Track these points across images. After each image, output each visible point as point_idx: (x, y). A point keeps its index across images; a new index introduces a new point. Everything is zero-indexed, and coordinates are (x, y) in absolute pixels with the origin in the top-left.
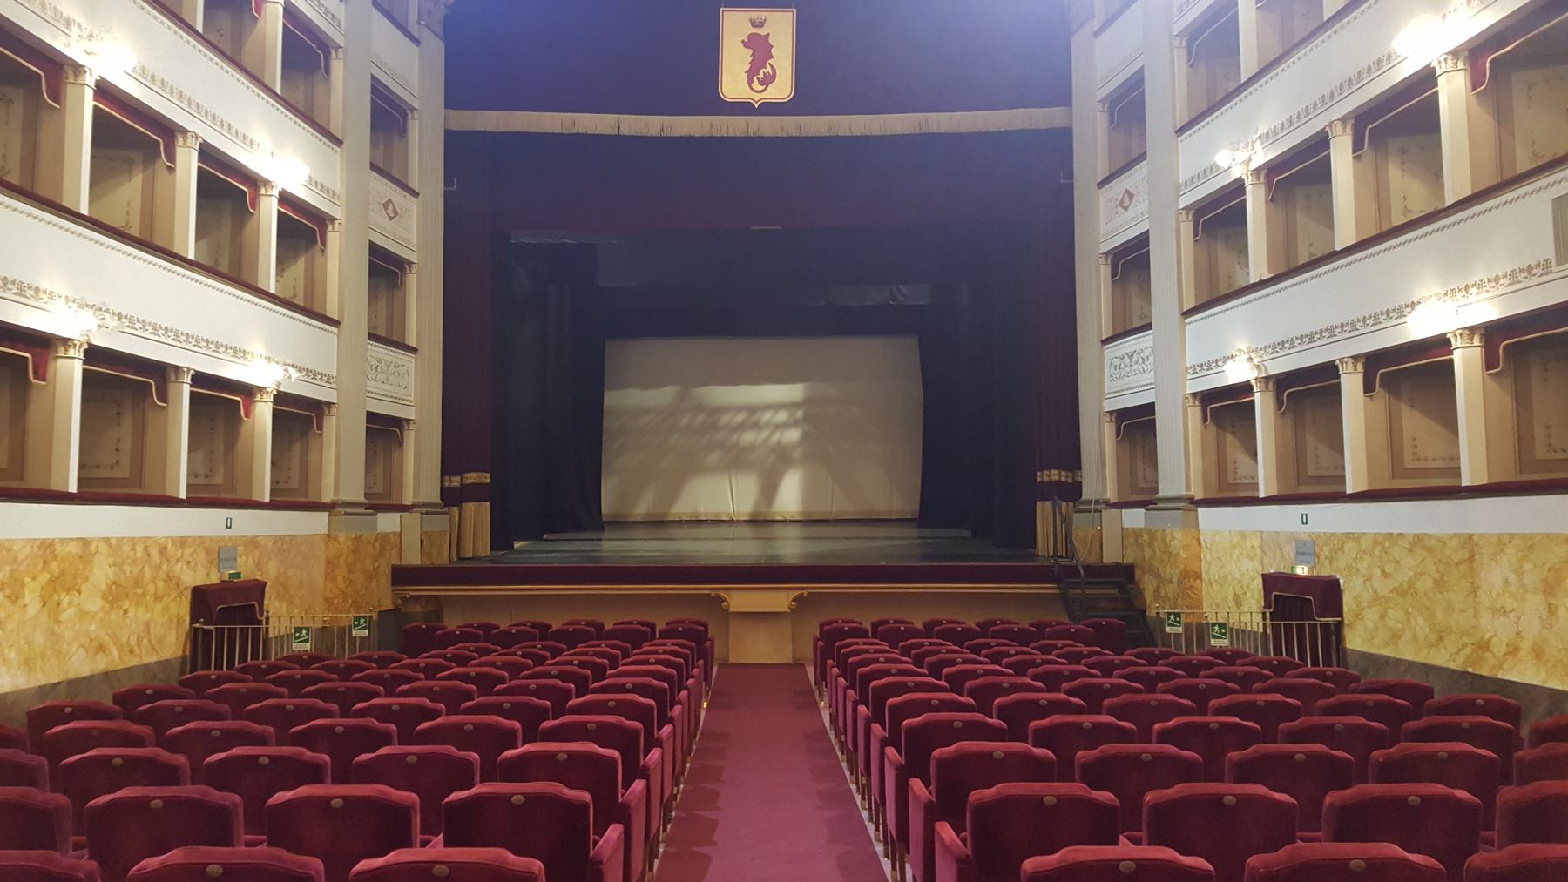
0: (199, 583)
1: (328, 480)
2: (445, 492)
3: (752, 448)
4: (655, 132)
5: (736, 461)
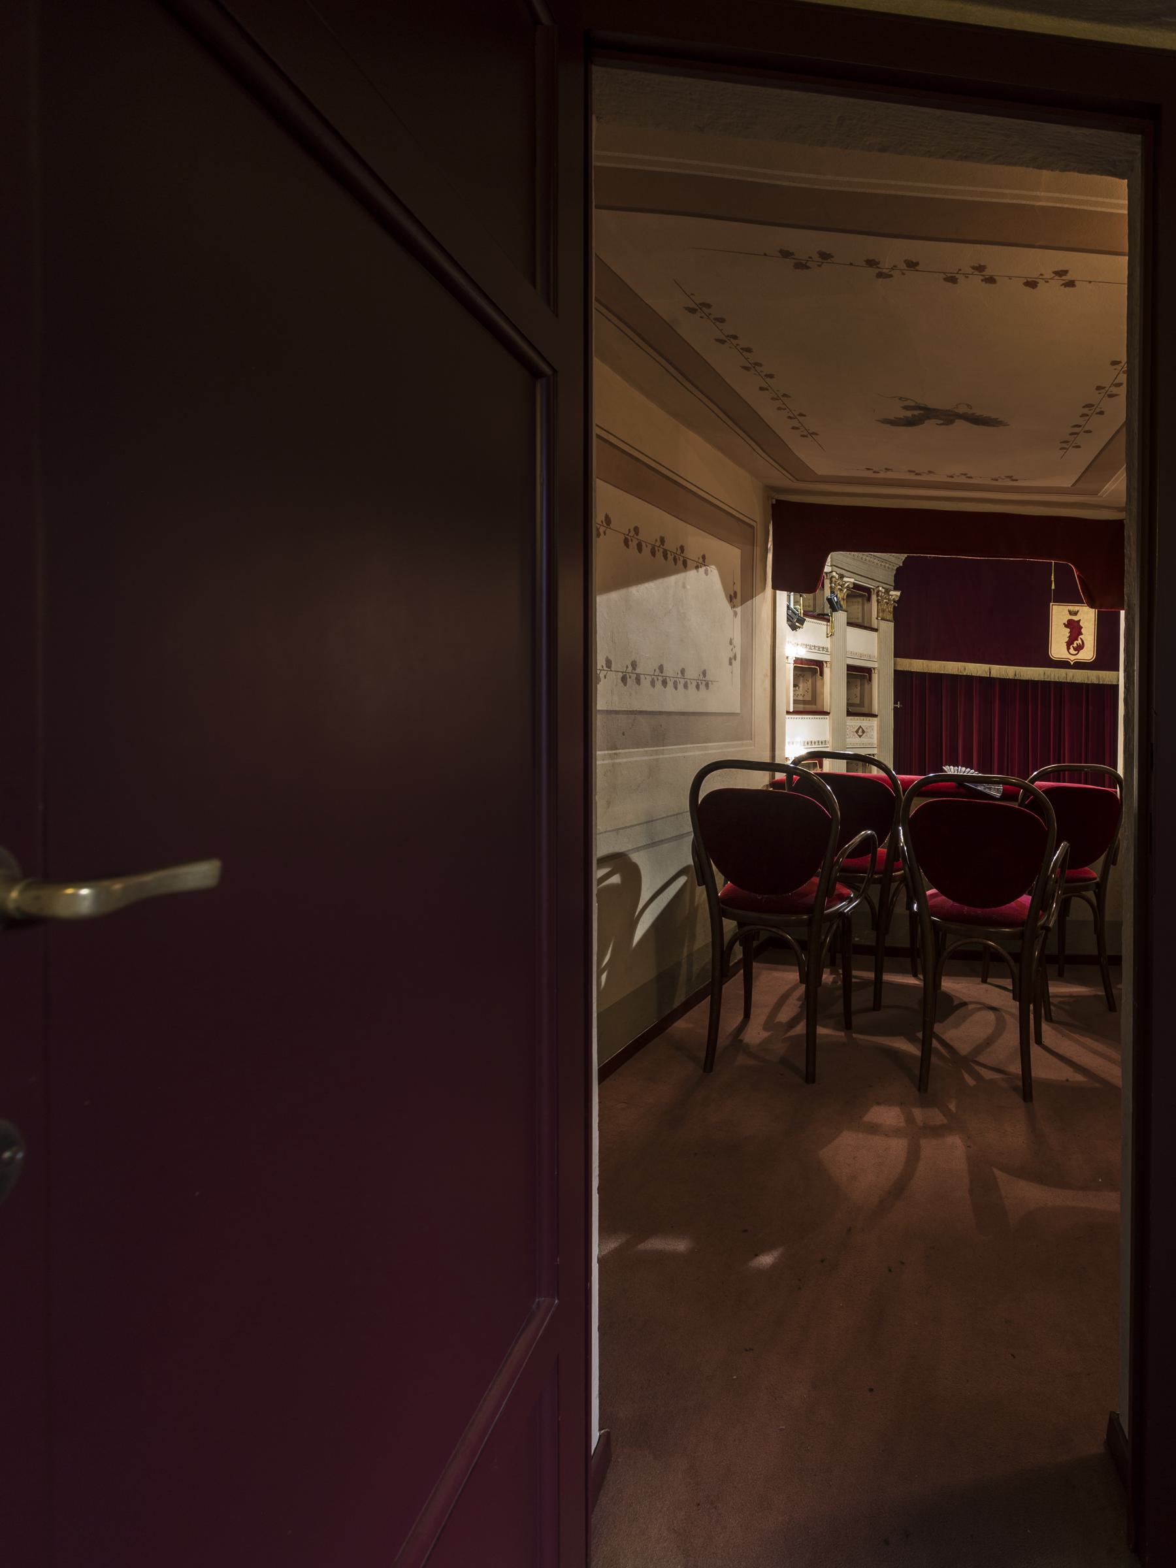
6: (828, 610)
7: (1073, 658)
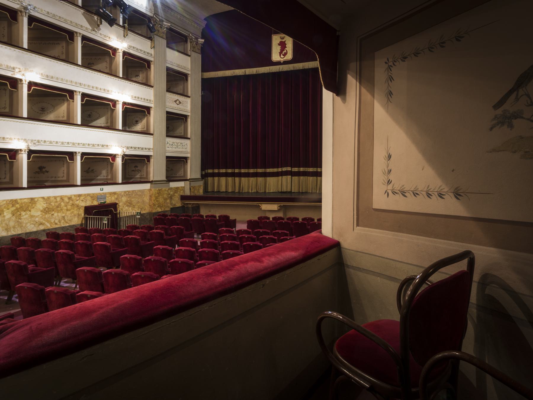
0: (88, 205)
1: (151, 175)
2: (202, 175)
4: (255, 73)
7: (282, 59)
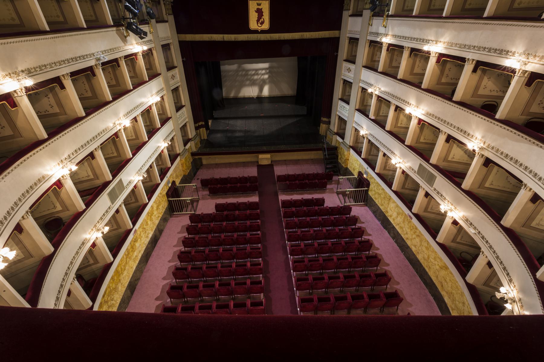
3: (257, 80)
5: (253, 83)
6: (146, 17)
